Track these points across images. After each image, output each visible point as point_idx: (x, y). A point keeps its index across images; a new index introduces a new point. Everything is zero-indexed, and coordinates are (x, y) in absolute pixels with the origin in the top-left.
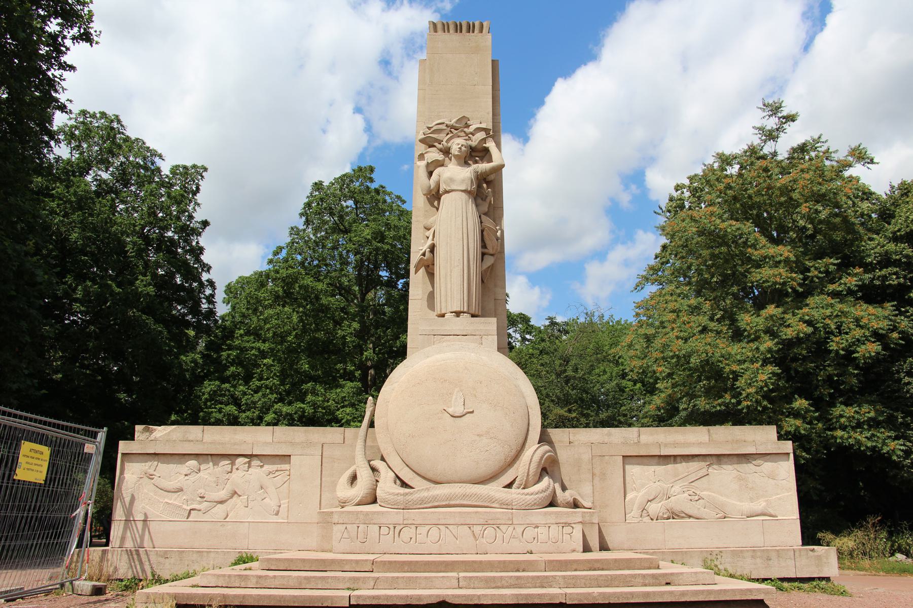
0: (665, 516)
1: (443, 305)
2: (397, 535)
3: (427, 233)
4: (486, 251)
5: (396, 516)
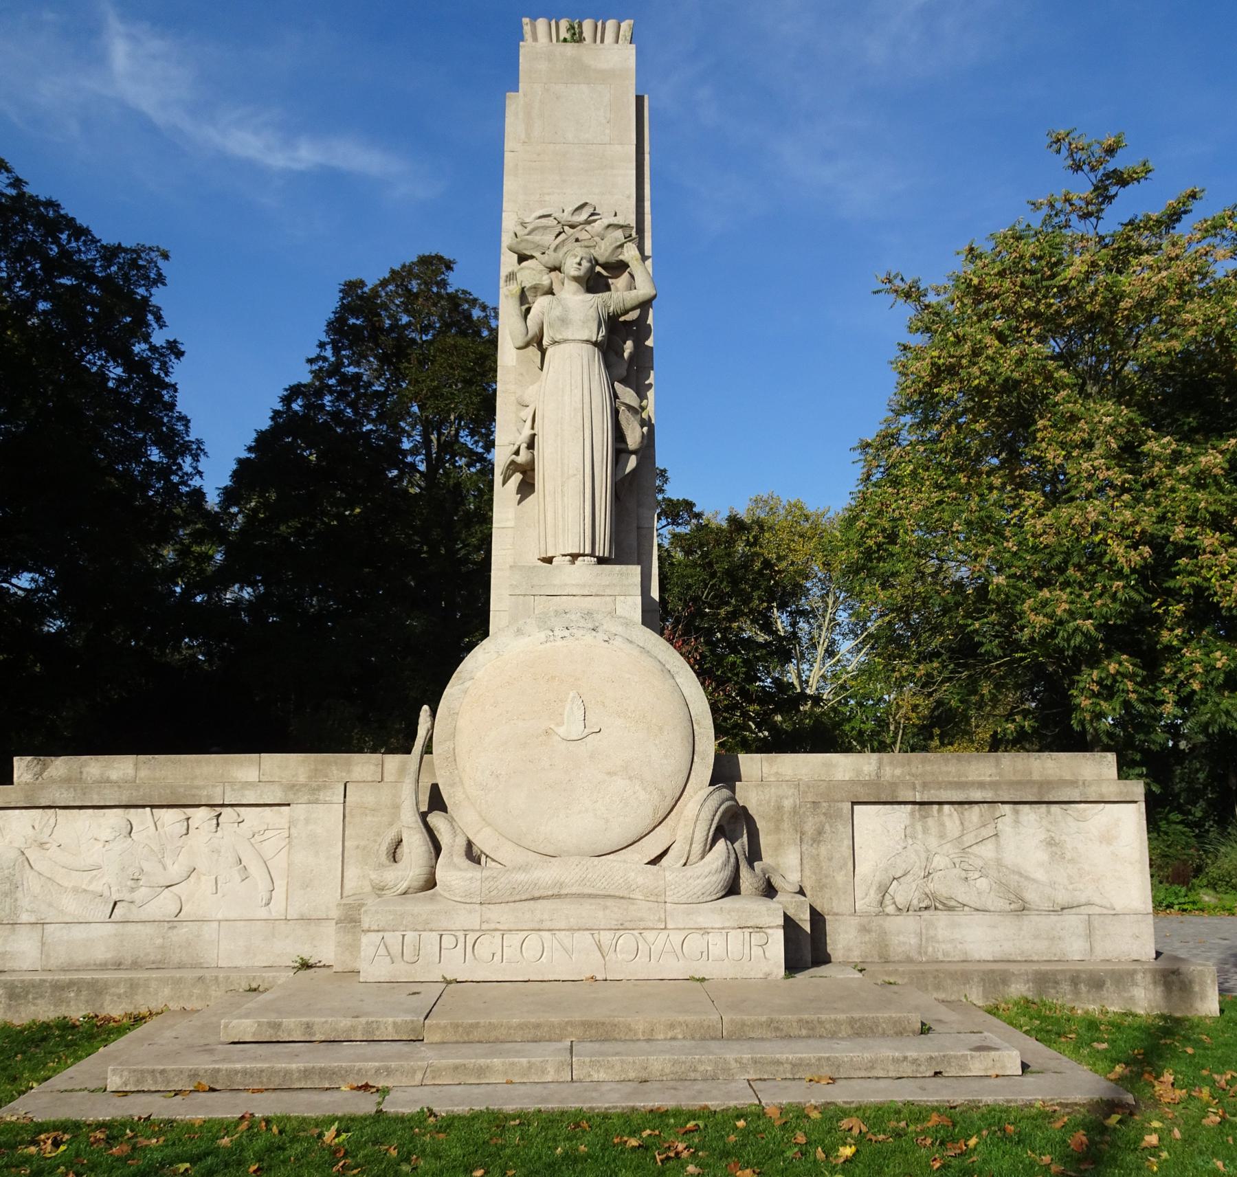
0: (923, 905)
1: (550, 540)
2: (469, 949)
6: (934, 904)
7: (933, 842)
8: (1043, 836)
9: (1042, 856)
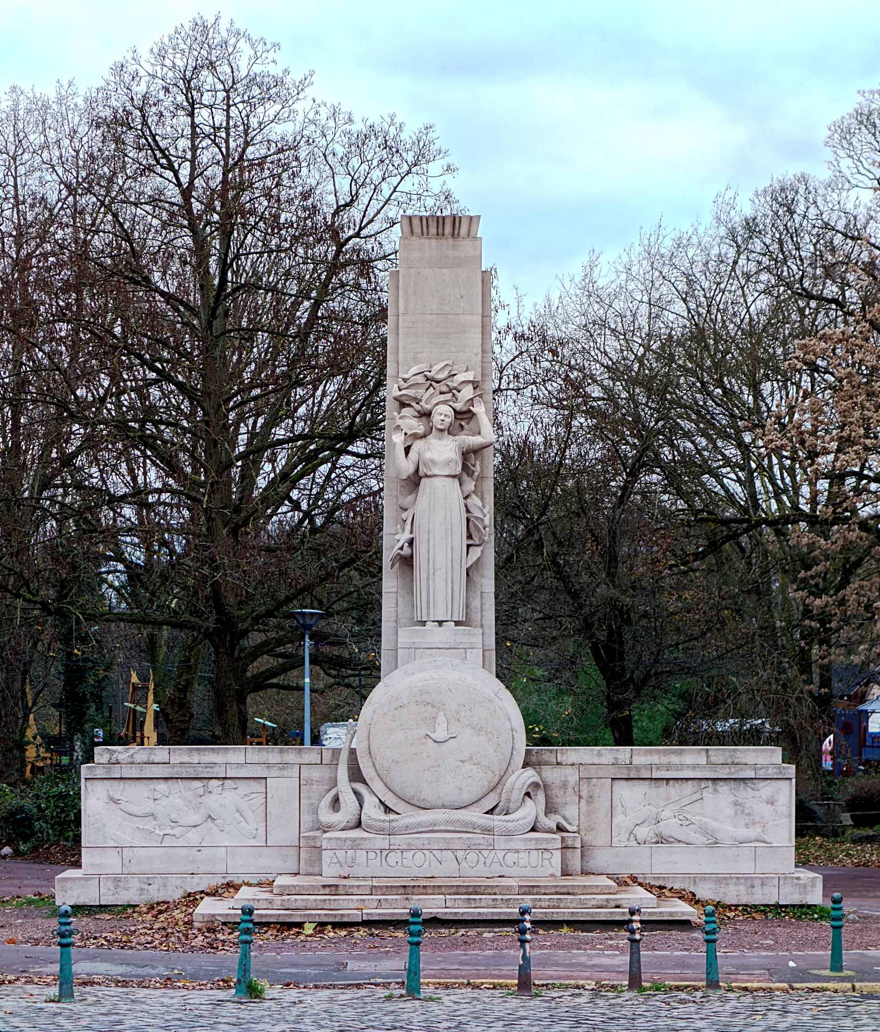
3: (404, 516)
4: (471, 542)
5: (381, 841)
6: (661, 840)
8: (732, 798)
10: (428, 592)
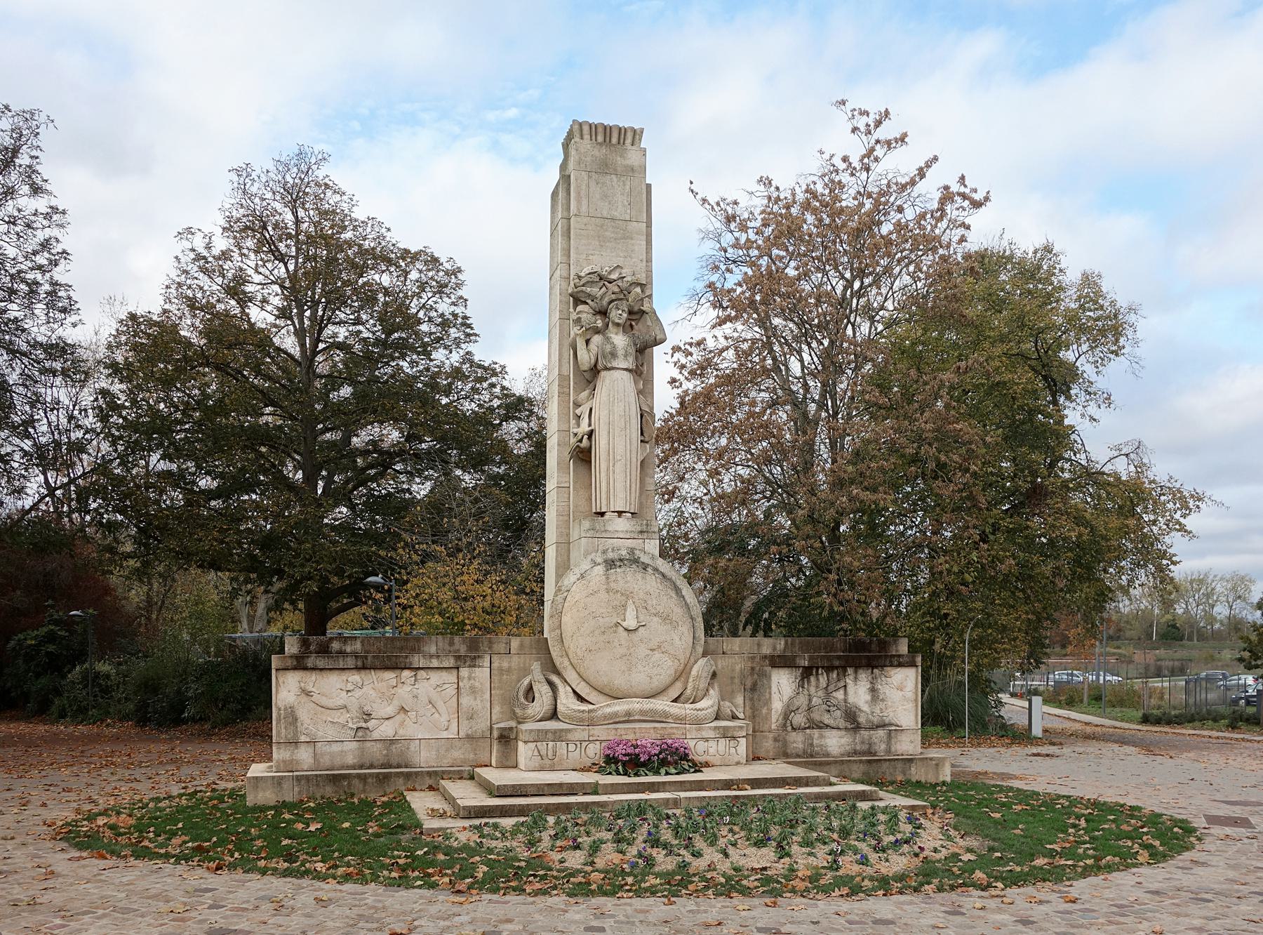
7: (813, 690)
9: (868, 697)
10: (608, 483)
